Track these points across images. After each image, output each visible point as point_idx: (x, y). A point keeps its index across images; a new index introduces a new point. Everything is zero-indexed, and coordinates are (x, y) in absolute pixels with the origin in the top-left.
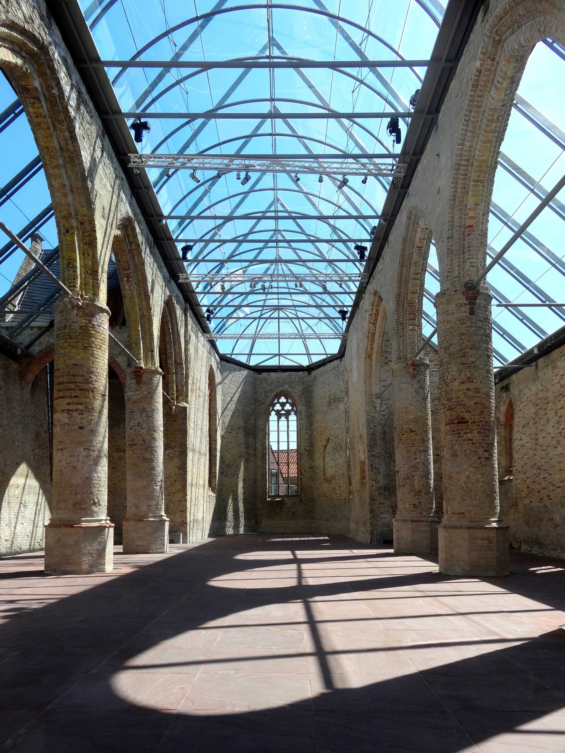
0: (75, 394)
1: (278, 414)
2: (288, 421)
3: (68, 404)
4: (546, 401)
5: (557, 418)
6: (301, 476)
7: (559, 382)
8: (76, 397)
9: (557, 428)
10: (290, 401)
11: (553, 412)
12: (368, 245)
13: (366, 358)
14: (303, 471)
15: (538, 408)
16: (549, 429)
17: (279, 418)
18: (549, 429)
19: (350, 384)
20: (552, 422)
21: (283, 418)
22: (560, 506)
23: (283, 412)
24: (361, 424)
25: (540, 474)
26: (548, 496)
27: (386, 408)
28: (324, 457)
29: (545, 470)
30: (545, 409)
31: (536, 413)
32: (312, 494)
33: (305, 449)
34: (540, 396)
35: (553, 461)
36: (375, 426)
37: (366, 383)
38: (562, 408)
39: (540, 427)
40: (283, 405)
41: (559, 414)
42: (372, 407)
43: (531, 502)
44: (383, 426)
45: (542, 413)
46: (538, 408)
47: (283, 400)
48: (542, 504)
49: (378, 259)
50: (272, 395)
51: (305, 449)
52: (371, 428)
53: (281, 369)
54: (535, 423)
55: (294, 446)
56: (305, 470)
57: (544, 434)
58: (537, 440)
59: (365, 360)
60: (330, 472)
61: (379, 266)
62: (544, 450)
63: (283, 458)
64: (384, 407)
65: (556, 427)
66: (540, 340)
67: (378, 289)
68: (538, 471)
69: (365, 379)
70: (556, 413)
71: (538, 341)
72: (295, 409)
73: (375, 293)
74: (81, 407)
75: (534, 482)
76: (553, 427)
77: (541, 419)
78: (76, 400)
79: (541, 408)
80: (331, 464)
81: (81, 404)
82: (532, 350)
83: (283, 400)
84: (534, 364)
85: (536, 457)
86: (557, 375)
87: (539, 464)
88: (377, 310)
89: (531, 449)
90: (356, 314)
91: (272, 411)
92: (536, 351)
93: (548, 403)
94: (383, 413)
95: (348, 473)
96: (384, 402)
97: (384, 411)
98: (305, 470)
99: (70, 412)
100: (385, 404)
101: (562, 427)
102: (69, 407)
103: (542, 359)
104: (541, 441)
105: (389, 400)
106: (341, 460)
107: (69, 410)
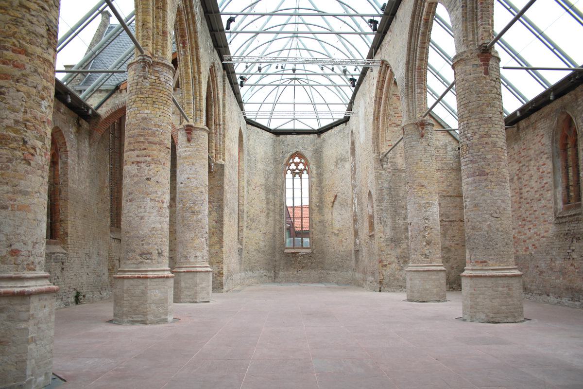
0: (144, 147)
1: (293, 172)
2: (301, 179)
3: (138, 156)
4: (528, 159)
5: (540, 173)
6: (313, 230)
7: (540, 141)
8: (145, 149)
9: (540, 183)
10: (303, 161)
11: (535, 168)
12: (379, 19)
13: (374, 120)
14: (314, 225)
15: (521, 165)
16: (533, 183)
17: (294, 176)
18: (533, 183)
19: (357, 145)
20: (535, 178)
21: (297, 176)
22: (545, 254)
23: (297, 171)
24: (369, 181)
25: (525, 225)
26: (533, 245)
27: (391, 165)
28: (332, 212)
29: (530, 221)
30: (528, 166)
31: (520, 169)
32: (322, 246)
33: (316, 205)
34: (523, 154)
35: (537, 213)
36: (382, 182)
37: (373, 143)
38: (544, 164)
39: (524, 182)
40: (297, 164)
41: (541, 170)
42: (380, 165)
43: (517, 251)
44: (389, 183)
45: (525, 169)
46: (521, 165)
47: (297, 160)
48: (528, 253)
49: (385, 33)
50: (289, 155)
51: (316, 205)
52: (379, 184)
53: (295, 132)
54: (519, 178)
55: (306, 202)
56: (316, 224)
57: (528, 189)
58: (521, 194)
59: (374, 122)
60: (337, 226)
61: (387, 38)
62: (528, 203)
63: (298, 213)
64: (390, 165)
65: (539, 181)
66: (522, 105)
67: (386, 59)
68: (524, 222)
69: (373, 139)
70: (538, 169)
71: (519, 105)
72: (307, 168)
73: (383, 62)
74: (148, 159)
75: (519, 232)
76: (536, 182)
77: (524, 174)
78: (144, 152)
79: (524, 165)
80: (339, 218)
81: (149, 156)
82: (515, 113)
83: (297, 160)
84: (516, 125)
85: (521, 209)
86: (538, 135)
87: (524, 216)
88: (383, 77)
89: (516, 202)
90: (364, 82)
91: (288, 170)
92: (518, 114)
93: (531, 160)
94: (389, 170)
95: (354, 226)
96: (389, 160)
98: (316, 224)
99: (139, 164)
100: (390, 162)
101: (544, 182)
102: (138, 159)
103: (523, 121)
104: (525, 195)
105: (394, 158)
106: (348, 215)
107: (138, 162)
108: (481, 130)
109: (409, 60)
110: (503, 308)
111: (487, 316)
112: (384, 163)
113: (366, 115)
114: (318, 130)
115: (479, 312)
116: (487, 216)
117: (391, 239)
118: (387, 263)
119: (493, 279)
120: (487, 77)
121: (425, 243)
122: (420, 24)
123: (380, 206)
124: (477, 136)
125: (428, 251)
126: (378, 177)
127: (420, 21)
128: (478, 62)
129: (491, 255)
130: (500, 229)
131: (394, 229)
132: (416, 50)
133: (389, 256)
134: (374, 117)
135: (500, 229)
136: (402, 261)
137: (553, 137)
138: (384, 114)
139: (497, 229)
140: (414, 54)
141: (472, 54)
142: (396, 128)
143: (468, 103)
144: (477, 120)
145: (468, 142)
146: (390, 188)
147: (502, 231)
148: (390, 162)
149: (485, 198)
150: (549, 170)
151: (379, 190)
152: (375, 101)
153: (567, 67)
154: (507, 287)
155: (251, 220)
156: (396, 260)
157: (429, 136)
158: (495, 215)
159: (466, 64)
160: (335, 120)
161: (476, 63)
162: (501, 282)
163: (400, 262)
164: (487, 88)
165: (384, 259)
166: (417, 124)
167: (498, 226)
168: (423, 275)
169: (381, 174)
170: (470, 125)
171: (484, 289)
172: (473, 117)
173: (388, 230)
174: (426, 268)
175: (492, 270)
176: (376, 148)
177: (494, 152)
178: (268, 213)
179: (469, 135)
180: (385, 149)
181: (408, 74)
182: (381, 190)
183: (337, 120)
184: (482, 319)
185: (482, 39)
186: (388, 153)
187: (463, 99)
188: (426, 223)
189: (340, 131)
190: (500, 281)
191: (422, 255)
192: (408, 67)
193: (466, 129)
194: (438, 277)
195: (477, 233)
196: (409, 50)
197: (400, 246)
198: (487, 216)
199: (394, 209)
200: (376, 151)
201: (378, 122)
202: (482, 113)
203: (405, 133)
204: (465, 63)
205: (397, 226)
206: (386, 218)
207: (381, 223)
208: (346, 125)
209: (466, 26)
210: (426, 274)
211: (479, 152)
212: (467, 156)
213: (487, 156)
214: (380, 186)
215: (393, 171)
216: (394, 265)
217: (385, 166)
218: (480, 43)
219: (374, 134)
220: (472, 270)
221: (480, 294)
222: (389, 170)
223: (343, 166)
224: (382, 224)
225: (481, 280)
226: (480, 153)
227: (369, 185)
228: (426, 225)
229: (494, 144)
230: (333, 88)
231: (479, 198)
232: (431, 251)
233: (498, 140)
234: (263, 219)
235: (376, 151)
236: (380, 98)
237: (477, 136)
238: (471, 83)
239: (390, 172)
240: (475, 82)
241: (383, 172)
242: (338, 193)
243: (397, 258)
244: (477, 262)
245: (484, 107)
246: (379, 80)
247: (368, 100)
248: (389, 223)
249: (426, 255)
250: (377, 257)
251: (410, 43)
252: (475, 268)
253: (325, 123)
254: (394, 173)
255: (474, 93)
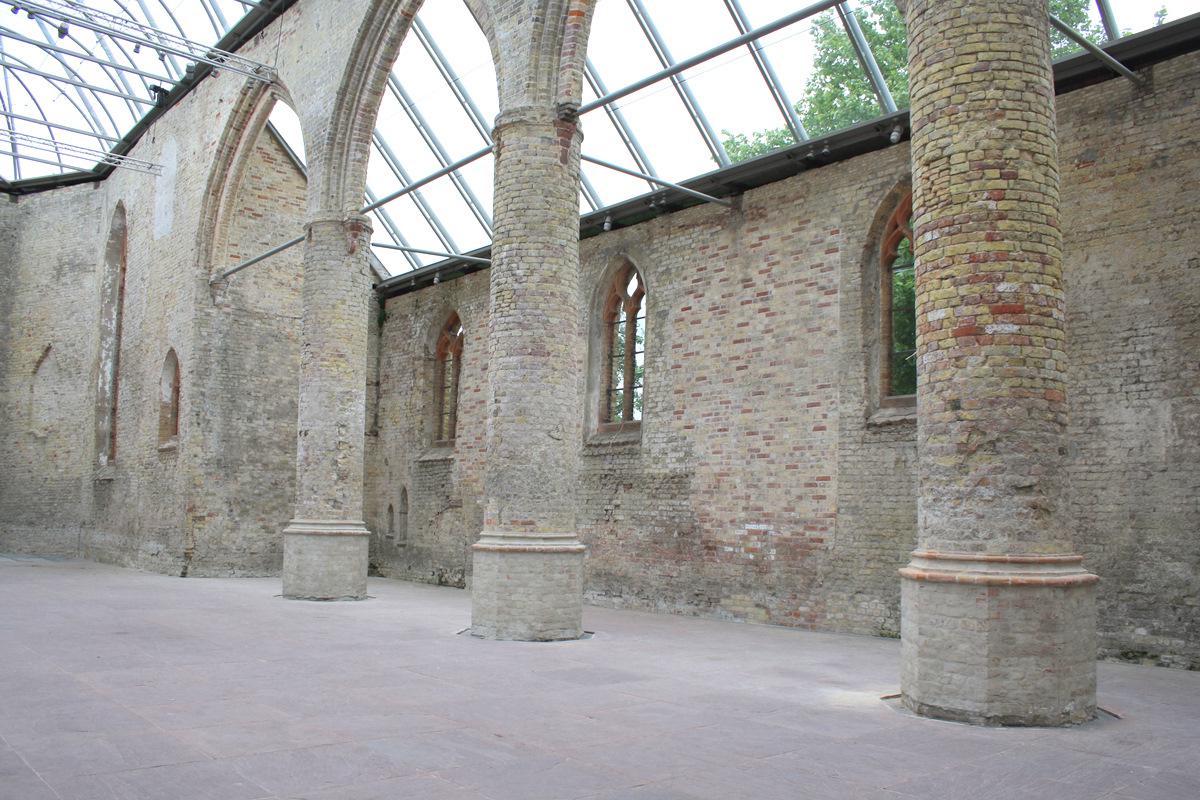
27: (234, 300)
37: (198, 244)
42: (208, 294)
44: (224, 337)
64: (230, 298)
96: (230, 287)
97: (228, 306)
100: (231, 292)
108: (545, 266)
109: (347, 86)
110: (559, 611)
111: (531, 628)
112: (219, 292)
114: (13, 184)
115: (515, 620)
116: (541, 435)
117: (219, 460)
118: (205, 514)
119: (546, 557)
120: (565, 167)
121: (335, 477)
122: (389, 20)
123: (199, 385)
124: (536, 277)
125: (340, 494)
126: (201, 322)
127: (393, 13)
128: (553, 134)
129: (543, 511)
130: (562, 462)
131: (226, 439)
132: (369, 69)
133: (210, 498)
134: (209, 186)
135: (562, 462)
136: (237, 511)
137: (594, 297)
138: (235, 186)
139: (557, 462)
140: (360, 76)
141: (543, 115)
142: (251, 221)
143: (525, 210)
144: (540, 246)
145: (516, 286)
146: (225, 350)
147: (564, 466)
148: (231, 292)
149: (540, 399)
150: (580, 357)
151: (200, 350)
152: (219, 152)
153: (640, 173)
154: (567, 571)
156: (225, 508)
157: (364, 253)
158: (556, 435)
159: (529, 132)
160: (66, 171)
161: (549, 135)
162: (558, 562)
163: (235, 513)
164: (562, 189)
165: (198, 504)
166: (343, 223)
167: (559, 455)
168: (327, 542)
169: (208, 314)
170: (524, 253)
171: (527, 575)
172: (531, 238)
173: (213, 442)
174: (335, 530)
175: (545, 539)
176: (204, 257)
177: (563, 314)
179: (520, 272)
180: (224, 263)
181: (339, 115)
182: (206, 350)
183: (75, 171)
184: (521, 635)
185: (568, 93)
186: (234, 272)
187: (516, 200)
188: (340, 434)
190: (558, 561)
191: (327, 501)
192: (342, 100)
193: (516, 260)
194: (357, 548)
195: (518, 467)
196: (352, 65)
197: (236, 478)
198: (541, 435)
199: (229, 396)
200: (202, 264)
201: (217, 199)
202: (550, 233)
203: (314, 238)
204: (528, 130)
205: (233, 432)
206: (212, 413)
207: (199, 424)
208: (96, 187)
209: (537, 60)
210: (335, 541)
211: (537, 308)
212: (511, 312)
213: (550, 319)
214: (204, 342)
215: (238, 312)
216: (220, 518)
217: (219, 299)
218: (562, 101)
219: (201, 224)
220: (504, 537)
221: (519, 586)
223: (76, 282)
224: (202, 425)
225: (522, 559)
226: (539, 312)
227: (173, 335)
228: (341, 438)
229: (565, 298)
230: (70, 90)
231: (528, 398)
232: (346, 493)
233: (570, 291)
235: (202, 264)
237: (536, 277)
238: (536, 172)
239: (228, 314)
240: (544, 171)
241: (214, 311)
242: (54, 342)
243: (228, 503)
244: (513, 522)
245: (555, 223)
246: (239, 107)
247: (194, 145)
248: (216, 426)
249: (335, 501)
250: (181, 500)
251: (357, 52)
252: (510, 534)
253: (31, 172)
254: (237, 318)
255: (539, 192)
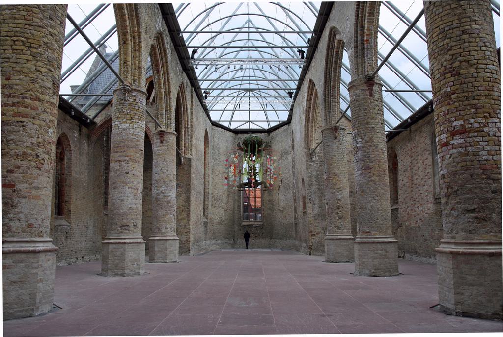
4: (417, 154)
5: (424, 165)
7: (424, 142)
11: (421, 161)
14: (264, 204)
15: (412, 159)
16: (420, 173)
18: (420, 173)
25: (415, 204)
29: (418, 201)
30: (417, 160)
31: (411, 162)
34: (413, 151)
35: (422, 195)
37: (305, 141)
38: (427, 159)
41: (425, 163)
43: (410, 224)
46: (412, 159)
54: (411, 169)
57: (417, 177)
58: (412, 180)
60: (282, 204)
62: (417, 188)
65: (424, 171)
67: (312, 79)
68: (414, 202)
70: (423, 162)
75: (412, 210)
76: (422, 172)
77: (414, 166)
79: (414, 159)
87: (415, 197)
89: (409, 187)
93: (418, 155)
98: (266, 203)
101: (427, 172)
113: (300, 120)
117: (319, 215)
123: (309, 190)
146: (317, 176)
151: (309, 177)
155: (215, 200)
156: (322, 231)
178: (229, 195)
182: (311, 177)
189: (284, 131)
217: (314, 159)
219: (305, 135)
222: (317, 162)
224: (312, 203)
234: (225, 199)
236: (310, 108)
241: (312, 164)
